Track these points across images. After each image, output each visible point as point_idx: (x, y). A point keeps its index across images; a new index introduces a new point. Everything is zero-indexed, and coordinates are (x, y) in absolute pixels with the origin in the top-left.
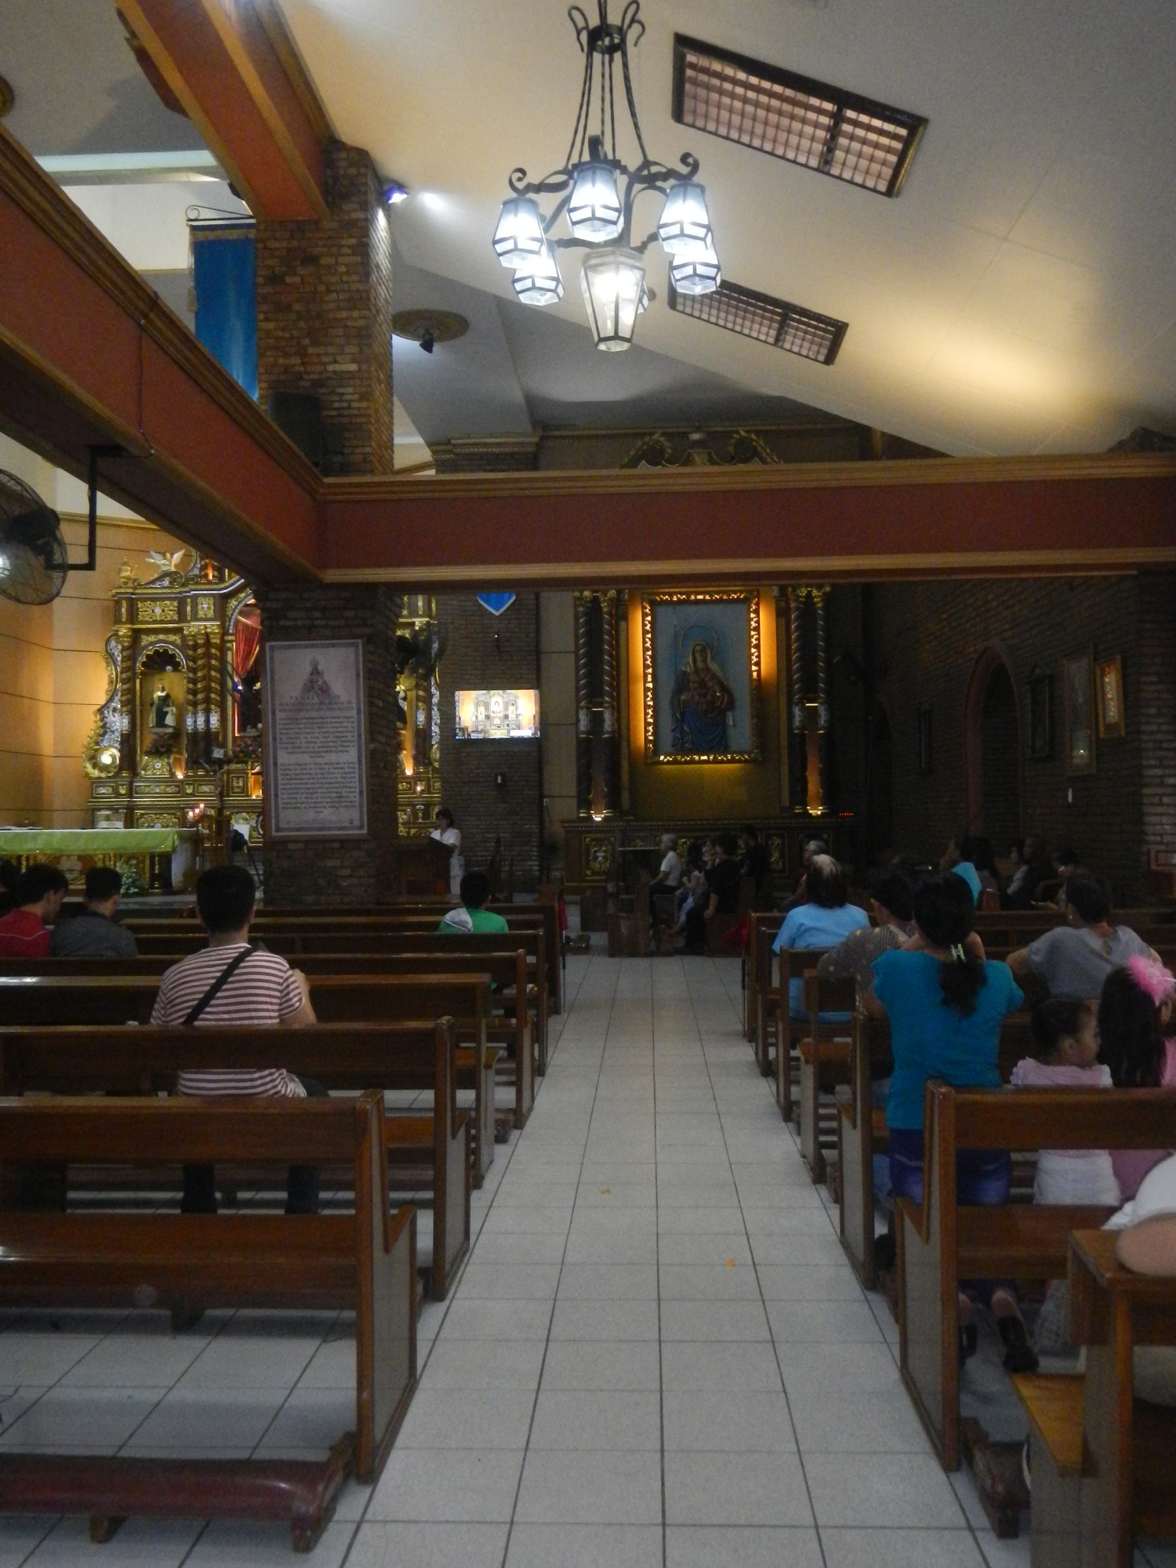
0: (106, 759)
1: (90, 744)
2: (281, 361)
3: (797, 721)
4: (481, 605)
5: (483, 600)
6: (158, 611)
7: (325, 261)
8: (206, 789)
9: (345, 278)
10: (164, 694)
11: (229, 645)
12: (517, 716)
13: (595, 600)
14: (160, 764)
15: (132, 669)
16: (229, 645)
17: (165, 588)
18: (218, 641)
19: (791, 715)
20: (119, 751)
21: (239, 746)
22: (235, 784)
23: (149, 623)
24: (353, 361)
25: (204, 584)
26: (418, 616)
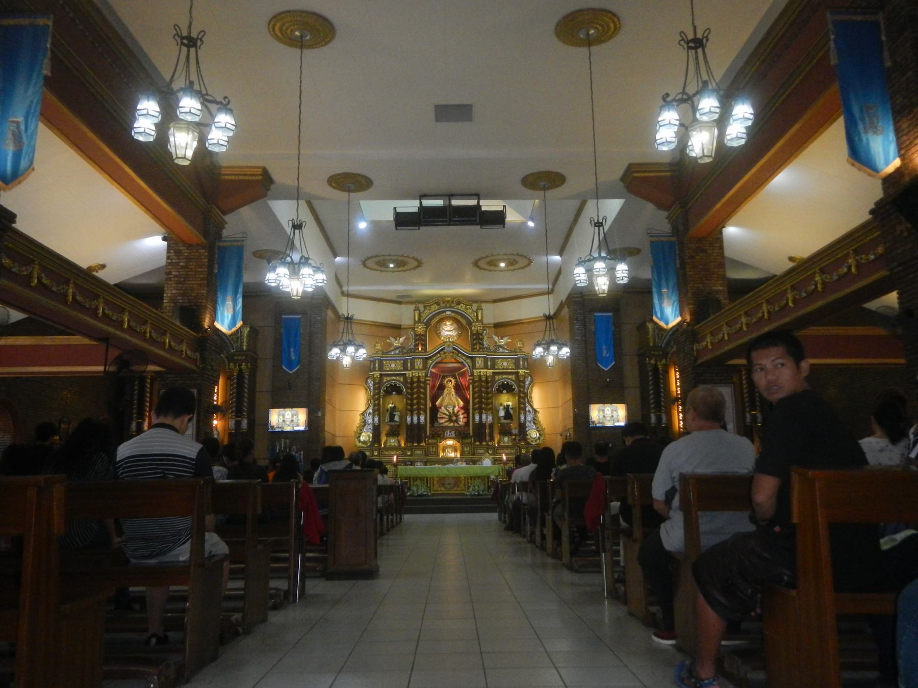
0: (362, 439)
1: (357, 430)
2: (696, 285)
3: (748, 419)
4: (598, 365)
5: (599, 363)
6: (393, 365)
7: (709, 251)
8: (418, 452)
9: (717, 258)
10: (393, 406)
11: (428, 382)
12: (617, 416)
15: (379, 393)
16: (428, 382)
18: (423, 380)
19: (745, 417)
21: (434, 431)
22: (431, 450)
23: (388, 371)
24: (721, 286)
26: (521, 369)
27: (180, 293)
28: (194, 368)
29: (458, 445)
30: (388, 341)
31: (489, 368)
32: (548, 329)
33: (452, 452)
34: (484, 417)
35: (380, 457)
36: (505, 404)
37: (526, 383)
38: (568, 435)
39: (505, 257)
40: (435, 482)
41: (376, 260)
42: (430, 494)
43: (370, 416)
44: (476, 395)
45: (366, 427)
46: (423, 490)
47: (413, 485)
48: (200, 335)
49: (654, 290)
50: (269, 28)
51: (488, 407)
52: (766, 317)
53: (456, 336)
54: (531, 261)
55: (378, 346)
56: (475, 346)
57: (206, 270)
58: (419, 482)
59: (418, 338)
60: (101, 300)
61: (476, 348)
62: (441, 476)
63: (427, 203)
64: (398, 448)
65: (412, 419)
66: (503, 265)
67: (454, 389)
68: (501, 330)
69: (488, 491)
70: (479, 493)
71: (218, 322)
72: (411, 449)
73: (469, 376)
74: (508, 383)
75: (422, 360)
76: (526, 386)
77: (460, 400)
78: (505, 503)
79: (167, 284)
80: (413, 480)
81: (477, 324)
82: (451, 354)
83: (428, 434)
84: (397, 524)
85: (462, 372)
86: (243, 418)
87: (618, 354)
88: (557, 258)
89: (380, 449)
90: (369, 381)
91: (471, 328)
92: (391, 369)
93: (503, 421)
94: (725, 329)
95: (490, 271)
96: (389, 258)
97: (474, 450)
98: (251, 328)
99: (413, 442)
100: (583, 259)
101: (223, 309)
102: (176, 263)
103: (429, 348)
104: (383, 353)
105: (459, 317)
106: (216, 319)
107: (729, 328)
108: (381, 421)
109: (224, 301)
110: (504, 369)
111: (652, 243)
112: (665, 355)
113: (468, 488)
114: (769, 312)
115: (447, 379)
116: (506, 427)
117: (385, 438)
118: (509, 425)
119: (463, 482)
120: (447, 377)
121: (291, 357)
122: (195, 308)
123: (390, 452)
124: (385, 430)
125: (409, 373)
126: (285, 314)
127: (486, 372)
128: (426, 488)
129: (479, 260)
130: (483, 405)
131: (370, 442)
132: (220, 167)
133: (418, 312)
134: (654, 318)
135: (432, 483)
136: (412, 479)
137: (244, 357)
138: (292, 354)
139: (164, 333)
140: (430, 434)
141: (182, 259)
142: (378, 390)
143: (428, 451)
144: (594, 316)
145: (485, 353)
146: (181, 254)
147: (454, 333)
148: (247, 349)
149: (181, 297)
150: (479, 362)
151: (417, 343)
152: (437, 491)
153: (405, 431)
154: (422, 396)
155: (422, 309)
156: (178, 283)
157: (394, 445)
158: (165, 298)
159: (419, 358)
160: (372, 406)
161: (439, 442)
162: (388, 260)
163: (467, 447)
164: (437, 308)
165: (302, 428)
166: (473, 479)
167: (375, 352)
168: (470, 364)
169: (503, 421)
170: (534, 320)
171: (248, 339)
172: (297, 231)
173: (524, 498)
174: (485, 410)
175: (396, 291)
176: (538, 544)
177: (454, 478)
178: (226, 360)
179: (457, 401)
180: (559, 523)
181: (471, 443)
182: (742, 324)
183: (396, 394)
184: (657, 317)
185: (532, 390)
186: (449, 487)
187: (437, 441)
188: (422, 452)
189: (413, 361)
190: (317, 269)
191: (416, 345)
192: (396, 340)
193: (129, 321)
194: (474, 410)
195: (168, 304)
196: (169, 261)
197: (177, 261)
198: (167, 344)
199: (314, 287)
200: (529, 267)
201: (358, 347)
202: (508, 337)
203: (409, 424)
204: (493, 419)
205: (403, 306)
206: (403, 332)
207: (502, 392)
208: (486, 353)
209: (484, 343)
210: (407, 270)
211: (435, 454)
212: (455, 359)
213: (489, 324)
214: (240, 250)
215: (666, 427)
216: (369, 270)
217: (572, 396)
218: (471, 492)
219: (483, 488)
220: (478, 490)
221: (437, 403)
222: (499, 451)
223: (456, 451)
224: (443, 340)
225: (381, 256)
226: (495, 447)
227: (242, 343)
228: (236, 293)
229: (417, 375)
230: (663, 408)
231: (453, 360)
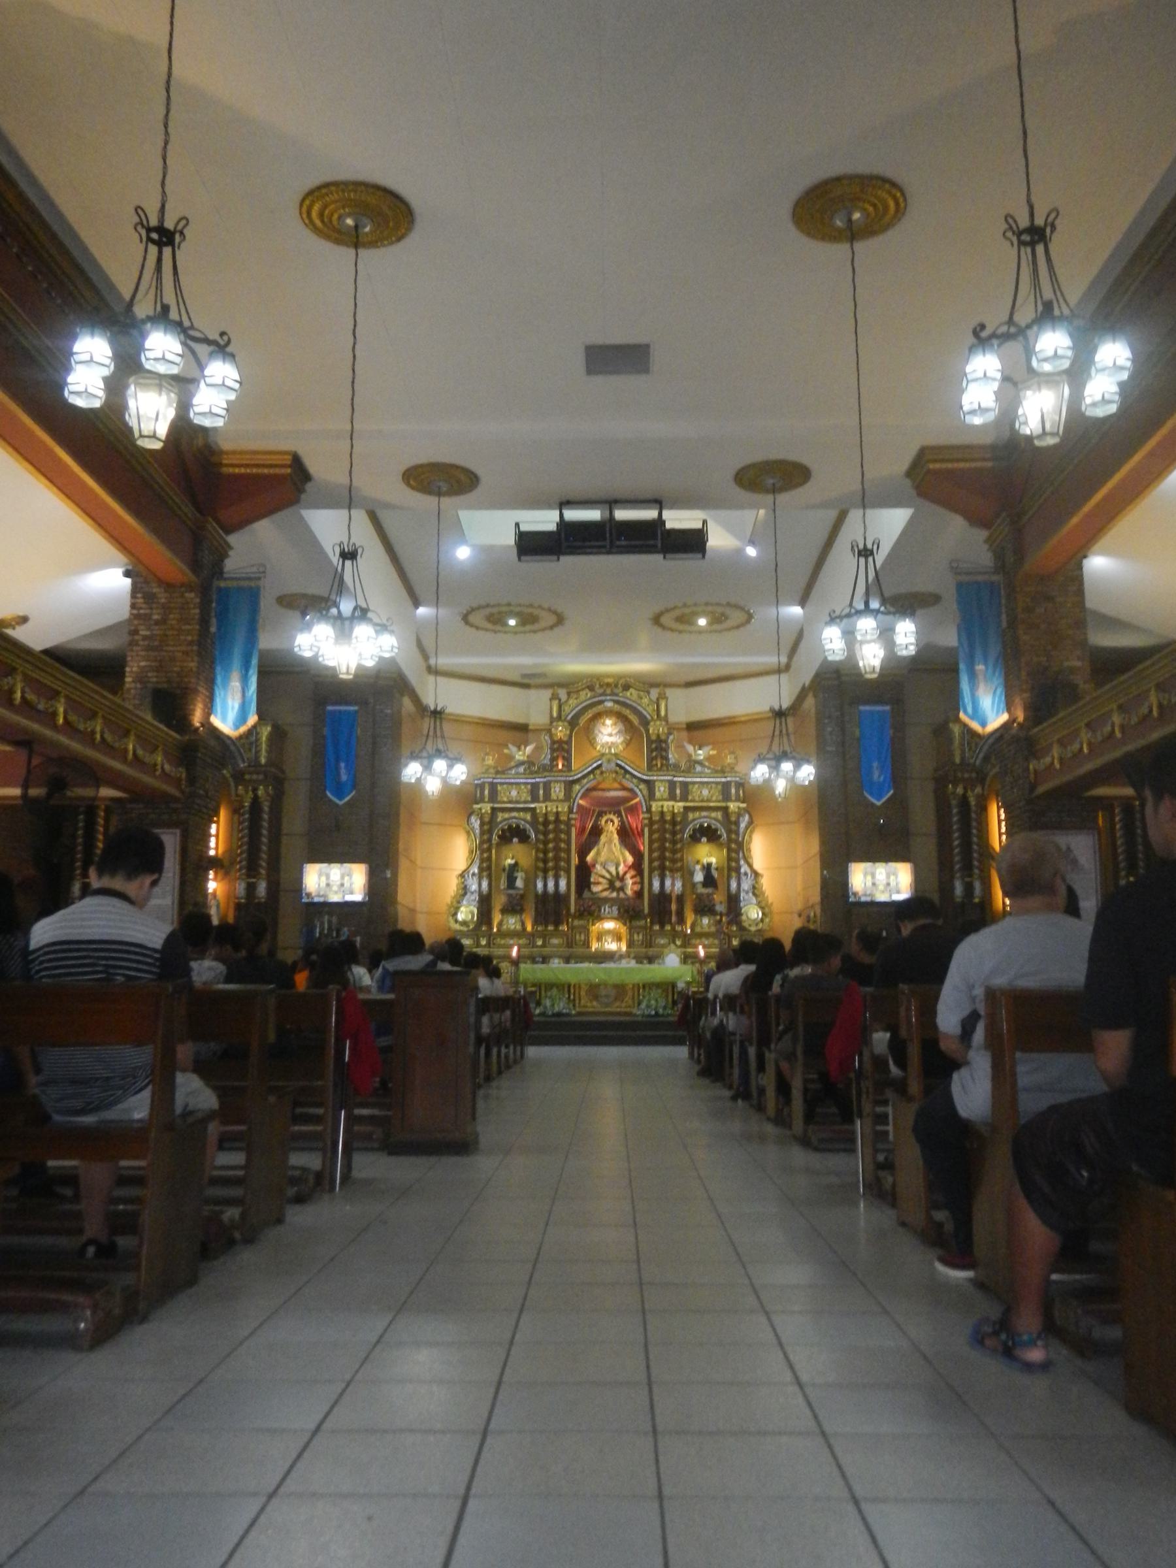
0: (460, 917)
1: (452, 903)
4: (865, 797)
6: (514, 793)
8: (555, 941)
13: (964, 798)
15: (490, 840)
16: (573, 822)
17: (521, 774)
22: (578, 937)
25: (556, 772)
27: (150, 666)
28: (177, 793)
29: (623, 930)
30: (506, 751)
31: (678, 798)
32: (777, 733)
34: (668, 883)
35: (489, 947)
36: (705, 861)
38: (812, 914)
39: (710, 608)
40: (583, 993)
41: (488, 611)
43: (475, 878)
44: (656, 845)
45: (467, 897)
47: (546, 997)
48: (187, 737)
49: (962, 666)
50: (301, 214)
51: (675, 866)
52: (1155, 713)
53: (622, 743)
54: (750, 617)
56: (654, 762)
57: (198, 627)
60: (19, 678)
61: (657, 765)
63: (572, 515)
64: (520, 934)
65: (545, 885)
66: (702, 622)
67: (618, 833)
71: (216, 716)
72: (544, 936)
73: (643, 812)
74: (709, 826)
76: (741, 830)
78: (700, 1031)
79: (132, 651)
81: (658, 723)
82: (614, 775)
83: (572, 910)
84: (515, 1062)
85: (632, 805)
87: (898, 778)
88: (796, 611)
90: (473, 819)
91: (647, 731)
94: (1085, 736)
95: (680, 632)
96: (504, 609)
99: (546, 926)
100: (837, 613)
101: (225, 695)
102: (145, 615)
104: (497, 772)
105: (627, 712)
106: (214, 711)
107: (1090, 734)
109: (226, 680)
110: (702, 801)
111: (960, 586)
112: (981, 779)
113: (639, 1004)
114: (1160, 706)
117: (500, 916)
119: (630, 993)
120: (606, 814)
121: (338, 774)
122: (178, 692)
123: (508, 940)
124: (499, 902)
125: (541, 807)
131: (474, 922)
132: (222, 452)
133: (557, 702)
134: (962, 715)
135: (577, 995)
137: (261, 777)
139: (127, 733)
140: (575, 909)
141: (157, 608)
144: (860, 712)
146: (155, 600)
147: (618, 739)
149: (155, 674)
150: (661, 790)
151: (555, 755)
153: (534, 906)
155: (563, 697)
156: (148, 648)
158: (127, 674)
159: (557, 782)
160: (478, 861)
162: (506, 613)
163: (638, 934)
165: (358, 897)
168: (645, 792)
169: (701, 890)
171: (268, 746)
172: (348, 563)
173: (732, 1022)
174: (671, 871)
176: (755, 1102)
177: (616, 986)
178: (231, 779)
179: (623, 854)
180: (785, 1065)
181: (645, 928)
182: (1113, 726)
184: (965, 712)
185: (750, 837)
188: (561, 941)
189: (547, 787)
190: (382, 628)
192: (519, 749)
193: (65, 712)
195: (133, 685)
196: (135, 612)
197: (148, 611)
198: (131, 753)
199: (377, 659)
200: (748, 626)
201: (453, 761)
202: (710, 747)
204: (683, 885)
205: (533, 693)
206: (530, 735)
208: (673, 773)
209: (670, 756)
212: (620, 783)
214: (253, 596)
215: (980, 902)
216: (473, 630)
217: (820, 848)
219: (664, 1004)
221: (589, 858)
222: (693, 941)
223: (619, 939)
224: (599, 751)
225: (493, 606)
226: (685, 935)
227: (258, 752)
228: (246, 666)
229: (555, 810)
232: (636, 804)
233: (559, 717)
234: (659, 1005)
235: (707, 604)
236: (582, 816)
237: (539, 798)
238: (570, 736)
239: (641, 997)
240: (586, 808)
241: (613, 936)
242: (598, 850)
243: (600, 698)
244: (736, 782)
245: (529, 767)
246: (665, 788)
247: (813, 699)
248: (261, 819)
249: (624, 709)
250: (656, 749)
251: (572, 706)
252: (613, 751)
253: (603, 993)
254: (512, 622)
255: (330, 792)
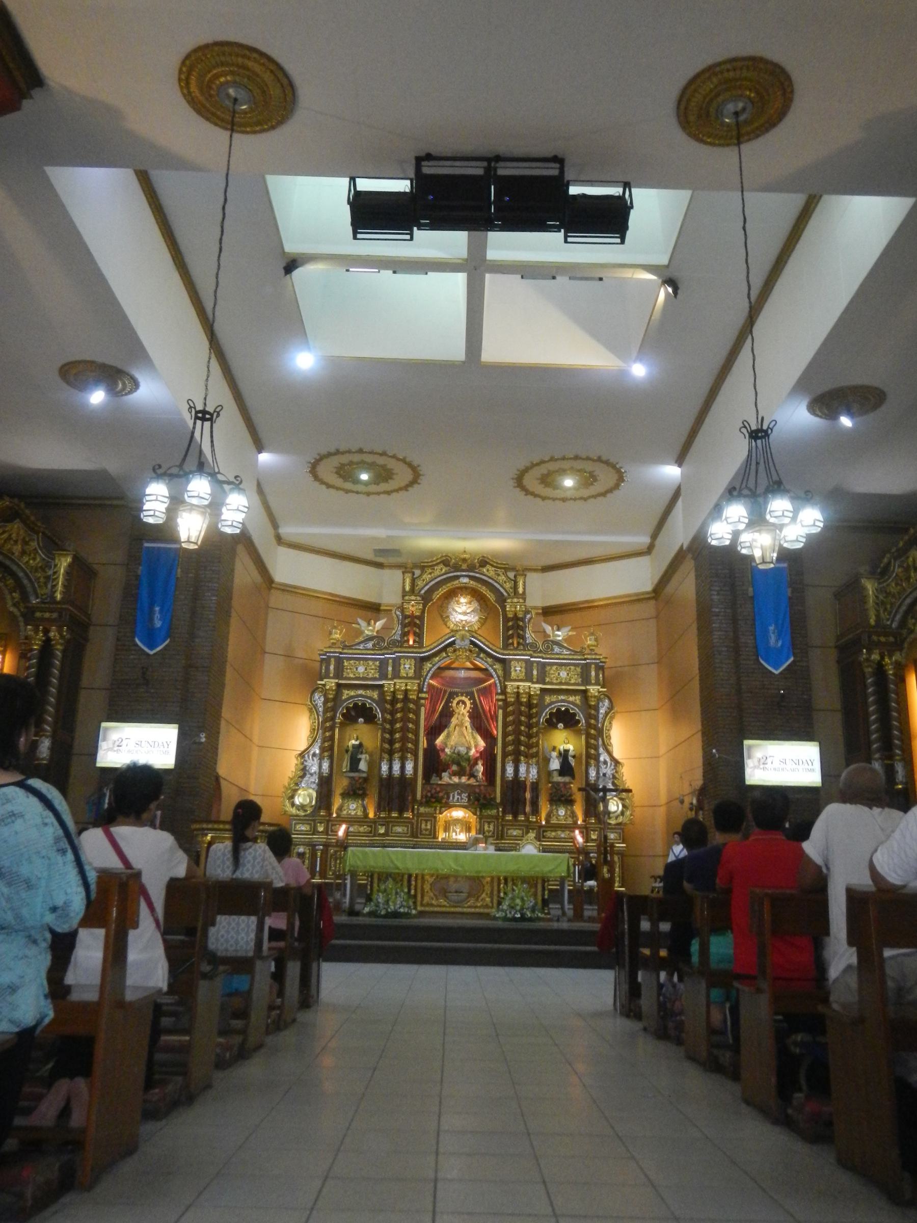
0: (298, 800)
1: (289, 785)
4: (761, 664)
5: (763, 660)
6: (361, 669)
8: (399, 829)
10: (357, 743)
11: (423, 701)
14: (355, 806)
15: (333, 719)
18: (414, 697)
20: (317, 793)
22: (423, 826)
23: (350, 679)
25: (406, 647)
26: (591, 684)
29: (473, 819)
31: (535, 680)
33: (460, 832)
34: (522, 769)
35: (327, 834)
36: (562, 748)
37: (601, 711)
39: (579, 465)
40: (427, 887)
41: (335, 461)
42: (414, 912)
43: (315, 758)
44: (510, 728)
46: (398, 902)
47: (378, 891)
51: (531, 751)
54: (621, 478)
55: (336, 633)
56: (511, 641)
58: (390, 884)
59: (409, 622)
61: (513, 644)
62: (440, 872)
64: (363, 820)
65: (390, 768)
67: (470, 717)
68: (557, 618)
69: (543, 912)
70: (523, 915)
72: (387, 823)
73: (497, 694)
74: (567, 710)
75: (413, 660)
76: (601, 716)
77: (479, 738)
80: (379, 880)
81: (515, 600)
85: (485, 688)
86: (43, 735)
88: (671, 472)
89: (328, 821)
90: (317, 696)
91: (504, 608)
92: (357, 675)
93: (557, 778)
95: (544, 498)
96: (356, 458)
97: (502, 831)
98: (76, 558)
99: (390, 811)
103: (426, 641)
105: (484, 590)
108: (334, 771)
110: (561, 683)
112: (898, 645)
113: (499, 903)
115: (457, 699)
116: (562, 789)
118: (568, 787)
119: (488, 889)
120: (457, 696)
124: (340, 785)
126: (149, 541)
127: (530, 688)
128: (405, 897)
129: (526, 470)
130: (522, 748)
133: (410, 575)
136: (376, 876)
137: (55, 615)
138: (157, 616)
140: (422, 797)
142: (332, 713)
143: (417, 831)
145: (528, 653)
147: (473, 619)
148: (62, 598)
150: (517, 669)
151: (406, 630)
152: (432, 905)
154: (411, 725)
155: (417, 572)
157: (356, 814)
159: (407, 658)
160: (319, 741)
161: (438, 812)
162: (357, 463)
163: (489, 823)
164: (444, 570)
166: (510, 884)
167: (331, 645)
168: (500, 672)
169: (557, 778)
170: (614, 601)
171: (67, 580)
174: (526, 757)
175: (375, 539)
178: (21, 619)
179: (474, 738)
181: (497, 817)
183: (365, 722)
185: (610, 723)
186: (454, 897)
187: (435, 810)
188: (406, 829)
189: (396, 663)
191: (405, 634)
194: (505, 755)
200: (616, 492)
203: (385, 776)
205: (387, 572)
206: (382, 614)
207: (556, 728)
209: (527, 636)
210: (392, 491)
211: (430, 835)
213: (535, 608)
216: (324, 487)
217: (703, 725)
218: (505, 911)
219: (531, 904)
220: (522, 909)
221: (439, 741)
222: (548, 834)
223: (468, 830)
225: (343, 453)
226: (541, 826)
227: (54, 586)
230: (897, 751)
231: (468, 665)
232: (490, 685)
233: (412, 591)
234: (526, 906)
235: (576, 458)
236: (432, 695)
237: (387, 675)
238: (423, 612)
239: (502, 895)
240: (437, 688)
241: (462, 824)
242: (447, 734)
243: (455, 574)
244: (596, 664)
245: (378, 644)
246: (521, 667)
247: (693, 562)
248: (51, 665)
249: (480, 586)
250: (512, 628)
251: (426, 580)
252: (467, 629)
253: (453, 886)
254: (364, 477)
255: (139, 640)
